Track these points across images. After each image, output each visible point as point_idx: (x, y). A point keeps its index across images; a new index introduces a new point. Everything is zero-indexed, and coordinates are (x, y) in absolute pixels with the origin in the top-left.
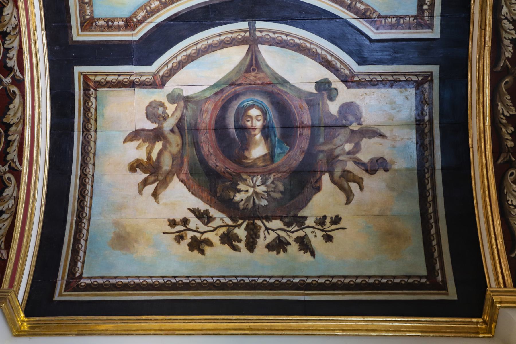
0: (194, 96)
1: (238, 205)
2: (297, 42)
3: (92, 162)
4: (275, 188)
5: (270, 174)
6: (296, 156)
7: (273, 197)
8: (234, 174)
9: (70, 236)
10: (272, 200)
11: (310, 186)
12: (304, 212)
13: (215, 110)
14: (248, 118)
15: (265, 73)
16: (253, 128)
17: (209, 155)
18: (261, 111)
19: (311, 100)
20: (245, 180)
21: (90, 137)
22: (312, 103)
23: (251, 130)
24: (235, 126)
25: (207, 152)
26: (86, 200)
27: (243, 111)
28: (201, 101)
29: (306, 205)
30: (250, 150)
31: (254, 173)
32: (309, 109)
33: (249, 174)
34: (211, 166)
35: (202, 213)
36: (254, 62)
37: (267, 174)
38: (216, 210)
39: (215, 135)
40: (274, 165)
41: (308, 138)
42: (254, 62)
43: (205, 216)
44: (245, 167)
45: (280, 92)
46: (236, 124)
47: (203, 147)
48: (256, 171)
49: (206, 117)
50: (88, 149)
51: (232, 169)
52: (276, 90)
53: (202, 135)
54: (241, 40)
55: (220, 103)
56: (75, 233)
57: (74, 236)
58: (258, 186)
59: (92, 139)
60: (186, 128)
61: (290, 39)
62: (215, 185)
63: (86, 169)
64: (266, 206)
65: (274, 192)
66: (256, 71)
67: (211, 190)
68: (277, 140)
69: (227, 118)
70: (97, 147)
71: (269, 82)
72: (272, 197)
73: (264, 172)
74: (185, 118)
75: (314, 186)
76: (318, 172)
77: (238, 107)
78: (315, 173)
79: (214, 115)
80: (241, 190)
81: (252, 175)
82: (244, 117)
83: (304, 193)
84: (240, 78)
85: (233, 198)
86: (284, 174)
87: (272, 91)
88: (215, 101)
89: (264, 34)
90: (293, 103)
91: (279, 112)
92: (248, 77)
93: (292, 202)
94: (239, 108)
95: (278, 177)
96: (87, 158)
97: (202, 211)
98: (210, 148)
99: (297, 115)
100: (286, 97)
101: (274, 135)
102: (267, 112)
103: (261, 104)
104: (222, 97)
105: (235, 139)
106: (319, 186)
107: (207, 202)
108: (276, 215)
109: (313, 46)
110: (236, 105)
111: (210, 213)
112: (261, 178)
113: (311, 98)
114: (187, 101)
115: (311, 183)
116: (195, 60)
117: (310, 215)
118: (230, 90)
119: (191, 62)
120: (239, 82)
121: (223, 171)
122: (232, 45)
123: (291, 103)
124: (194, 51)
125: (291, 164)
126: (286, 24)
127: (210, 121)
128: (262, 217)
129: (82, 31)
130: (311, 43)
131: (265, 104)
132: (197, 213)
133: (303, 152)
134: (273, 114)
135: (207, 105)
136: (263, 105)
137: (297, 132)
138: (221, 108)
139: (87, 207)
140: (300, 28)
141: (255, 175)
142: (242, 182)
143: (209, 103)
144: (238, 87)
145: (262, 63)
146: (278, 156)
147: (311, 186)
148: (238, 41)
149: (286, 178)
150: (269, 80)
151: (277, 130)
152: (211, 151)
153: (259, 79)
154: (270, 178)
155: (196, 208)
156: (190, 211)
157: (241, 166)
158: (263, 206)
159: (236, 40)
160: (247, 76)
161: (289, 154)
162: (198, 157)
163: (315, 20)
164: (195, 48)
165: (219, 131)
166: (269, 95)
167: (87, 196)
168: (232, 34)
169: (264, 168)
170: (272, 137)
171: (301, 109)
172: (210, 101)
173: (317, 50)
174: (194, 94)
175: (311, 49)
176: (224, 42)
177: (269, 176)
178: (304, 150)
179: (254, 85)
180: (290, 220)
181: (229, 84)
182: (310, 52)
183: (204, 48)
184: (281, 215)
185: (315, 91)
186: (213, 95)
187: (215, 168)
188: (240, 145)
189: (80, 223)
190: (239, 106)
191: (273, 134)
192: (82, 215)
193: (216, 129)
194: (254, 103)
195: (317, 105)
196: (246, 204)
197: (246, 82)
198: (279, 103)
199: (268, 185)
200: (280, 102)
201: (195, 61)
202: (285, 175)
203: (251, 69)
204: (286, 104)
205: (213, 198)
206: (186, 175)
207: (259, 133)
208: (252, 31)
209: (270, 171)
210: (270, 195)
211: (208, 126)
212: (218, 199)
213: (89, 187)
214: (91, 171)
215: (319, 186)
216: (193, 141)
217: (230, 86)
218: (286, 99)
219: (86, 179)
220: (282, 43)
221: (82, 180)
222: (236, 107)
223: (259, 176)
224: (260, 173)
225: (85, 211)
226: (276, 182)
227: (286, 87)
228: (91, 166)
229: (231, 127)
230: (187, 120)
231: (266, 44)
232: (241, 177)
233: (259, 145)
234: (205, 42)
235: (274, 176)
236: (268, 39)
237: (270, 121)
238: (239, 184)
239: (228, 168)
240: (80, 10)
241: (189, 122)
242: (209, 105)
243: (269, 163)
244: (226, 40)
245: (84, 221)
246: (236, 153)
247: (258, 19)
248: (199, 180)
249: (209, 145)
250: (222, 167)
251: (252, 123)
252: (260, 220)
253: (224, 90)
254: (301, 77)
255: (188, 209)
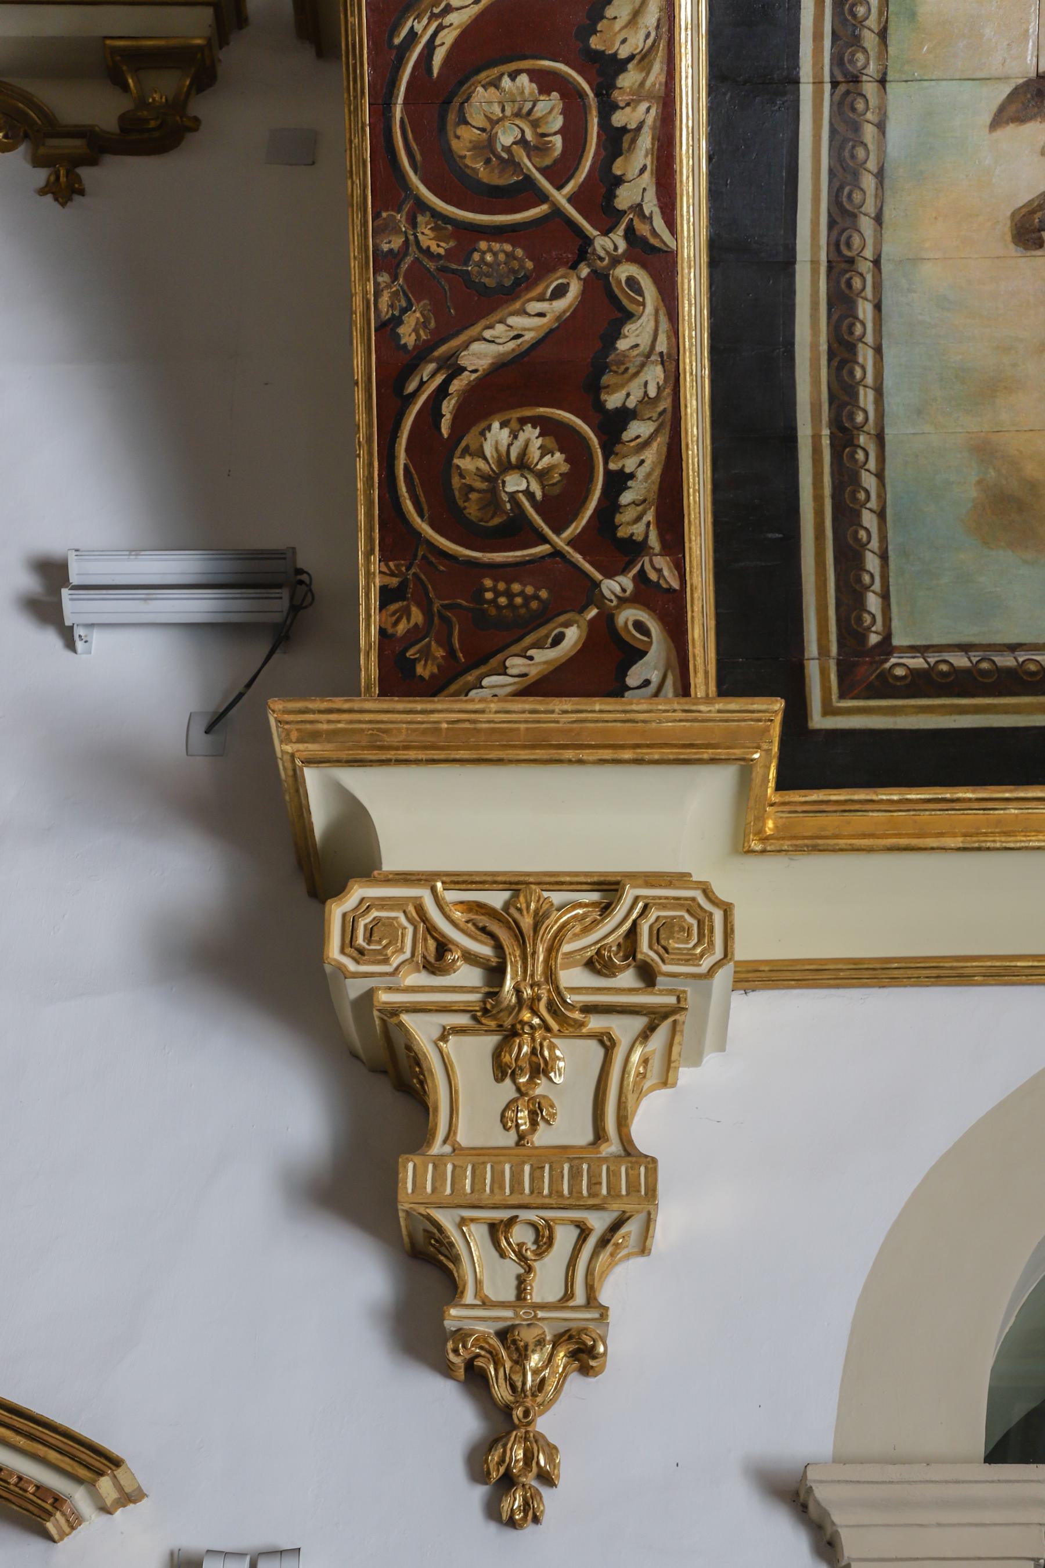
3: (870, 207)
21: (860, 105)
26: (861, 360)
50: (853, 156)
57: (833, 497)
59: (869, 116)
63: (850, 237)
70: (890, 149)
139: (865, 386)
167: (860, 345)
192: (851, 417)
213: (865, 310)
214: (870, 242)
219: (851, 278)
221: (838, 282)
225: (862, 404)
228: (866, 224)
245: (862, 439)
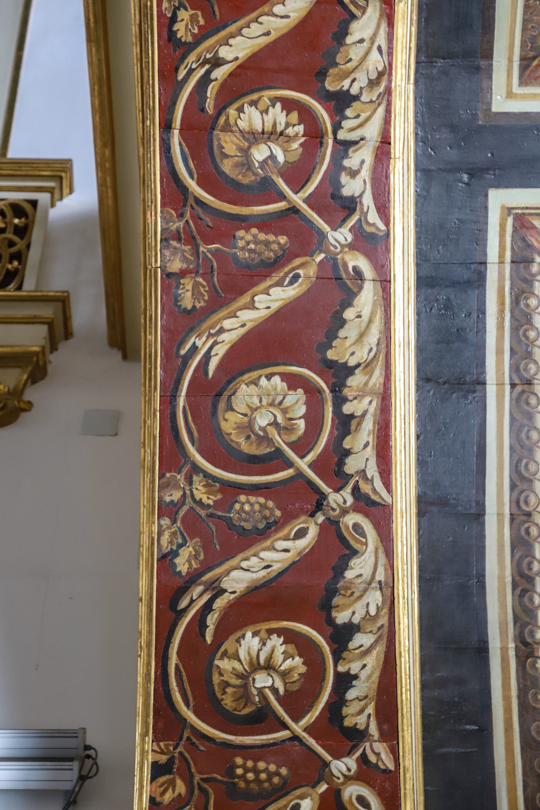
9: (507, 698)
56: (520, 690)
57: (519, 697)
63: (527, 497)
96: (526, 466)
129: (523, 82)
189: (529, 660)
219: (529, 527)
221: (519, 530)
240: (525, 22)
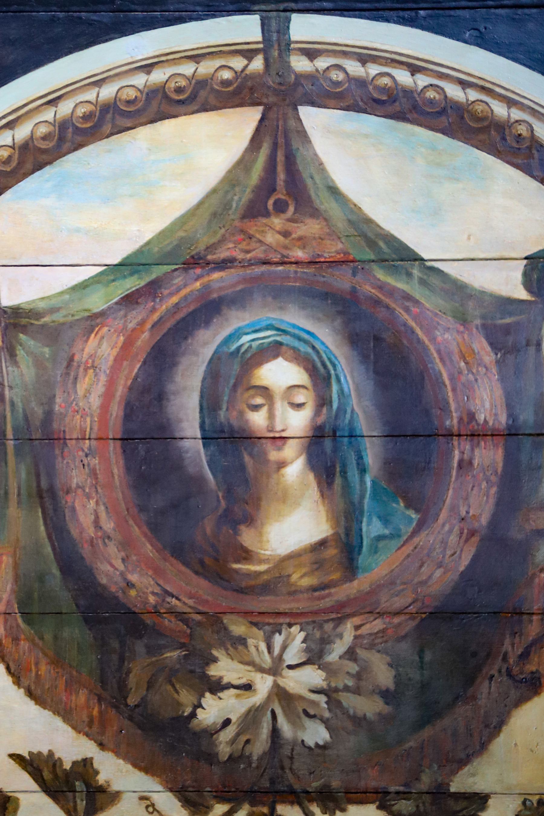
0: (42, 305)
1: (213, 744)
2: (456, 98)
4: (358, 676)
5: (339, 621)
6: (445, 549)
7: (351, 712)
8: (198, 617)
10: (349, 725)
11: (500, 671)
12: (473, 775)
13: (125, 363)
14: (253, 397)
15: (326, 220)
16: (274, 438)
17: (100, 542)
18: (306, 369)
19: (507, 330)
20: (242, 641)
22: (510, 340)
23: (268, 446)
24: (202, 427)
25: (91, 531)
27: (236, 368)
28: (72, 325)
29: (483, 746)
30: (262, 524)
31: (279, 614)
32: (497, 362)
33: (256, 619)
34: (104, 587)
35: (67, 774)
36: (281, 176)
37: (327, 621)
38: (121, 761)
39: (122, 462)
40: (355, 583)
41: (494, 479)
42: (281, 176)
43: (79, 785)
44: (241, 591)
45: (383, 298)
46: (207, 421)
47: (73, 509)
48: (284, 607)
49: (88, 392)
51: (191, 596)
52: (368, 289)
53: (74, 461)
54: (231, 89)
55: (146, 335)
58: (290, 667)
60: (10, 434)
61: (426, 84)
62: (122, 659)
64: (324, 747)
65: (357, 691)
66: (291, 209)
67: (103, 682)
68: (369, 484)
69: (172, 397)
71: (339, 257)
72: (345, 712)
73: (316, 613)
74: (7, 392)
75: (516, 670)
76: (533, 614)
77: (215, 352)
78: (520, 622)
79: (122, 382)
80: (225, 680)
81: (269, 624)
82: (239, 391)
83: (474, 698)
84: (224, 236)
85: (193, 715)
86: (396, 620)
87: (354, 292)
88: (125, 327)
89: (322, 63)
90: (433, 340)
91: (376, 372)
92: (258, 236)
93: (427, 732)
94: (219, 359)
95: (371, 634)
97: (67, 766)
98: (103, 515)
99: (449, 388)
100: (406, 316)
101: (358, 464)
102: (332, 372)
103: (305, 342)
104: (154, 310)
105: (200, 480)
106: (537, 671)
107: (87, 729)
108: (362, 784)
109: (516, 114)
110: (206, 344)
111: (97, 773)
112: (302, 635)
113: (508, 320)
114: (15, 325)
115: (505, 658)
116: (50, 163)
117: (498, 789)
118: (185, 286)
119: (33, 172)
120: (223, 254)
121: (155, 607)
122: (196, 108)
123: (427, 342)
124: (43, 130)
125: (423, 583)
126: (412, 26)
127: (105, 407)
128: (307, 792)
130: (511, 103)
131: (323, 343)
132: (47, 775)
133: (472, 533)
134: (354, 382)
135: (93, 341)
136: (314, 348)
137: (449, 453)
138: (149, 354)
140: (466, 42)
141: (281, 624)
142: (227, 650)
143: (103, 337)
144: (216, 275)
145: (312, 178)
146: (374, 550)
147: (504, 670)
148: (217, 91)
149: (404, 637)
150: (340, 246)
151: (368, 445)
152: (108, 525)
153: (303, 242)
154: (341, 636)
155: (45, 752)
156: (20, 765)
157: (225, 589)
158: (310, 748)
159: (212, 89)
160: (251, 232)
161: (416, 540)
162: (54, 549)
163: (527, 11)
164: (49, 115)
165: (142, 448)
166: (340, 308)
168: (198, 63)
169: (317, 594)
170: (349, 474)
171: (467, 363)
172: (105, 329)
173: (532, 130)
174: (43, 299)
175: (510, 127)
176: (166, 97)
177: (335, 628)
178: (476, 525)
179: (281, 268)
180: (418, 806)
181: (182, 260)
182: (504, 139)
183: (86, 117)
184: (383, 784)
185: (522, 294)
186: (116, 303)
187: (120, 594)
188: (223, 503)
190: (219, 346)
191: (354, 462)
193: (127, 439)
194: (278, 338)
195: (532, 350)
196: (243, 738)
197: (249, 256)
198: (377, 339)
199: (330, 663)
200: (384, 335)
201: (47, 170)
202: (400, 624)
203: (271, 202)
204: (405, 342)
205: (113, 713)
206: (6, 621)
207: (297, 458)
208: (276, 54)
209: (340, 606)
210: (339, 704)
211: (96, 428)
212: (131, 718)
215: (537, 671)
216: (35, 485)
217: (186, 270)
218: (405, 325)
220: (395, 101)
222: (208, 352)
223: (295, 629)
224: (302, 614)
226: (362, 653)
227: (409, 275)
229: (189, 433)
230: (13, 404)
231: (332, 102)
232: (226, 629)
233: (299, 504)
234: (90, 95)
235: (357, 628)
236: (337, 84)
237: (341, 410)
238: (215, 660)
239: (173, 596)
241: (21, 410)
242: (99, 345)
243: (336, 576)
244: (172, 85)
246: (205, 534)
247: (300, 6)
248: (56, 637)
249: (97, 503)
250: (150, 589)
251: (271, 416)
252: (300, 804)
253: (160, 287)
254: (469, 238)
255: (11, 756)
